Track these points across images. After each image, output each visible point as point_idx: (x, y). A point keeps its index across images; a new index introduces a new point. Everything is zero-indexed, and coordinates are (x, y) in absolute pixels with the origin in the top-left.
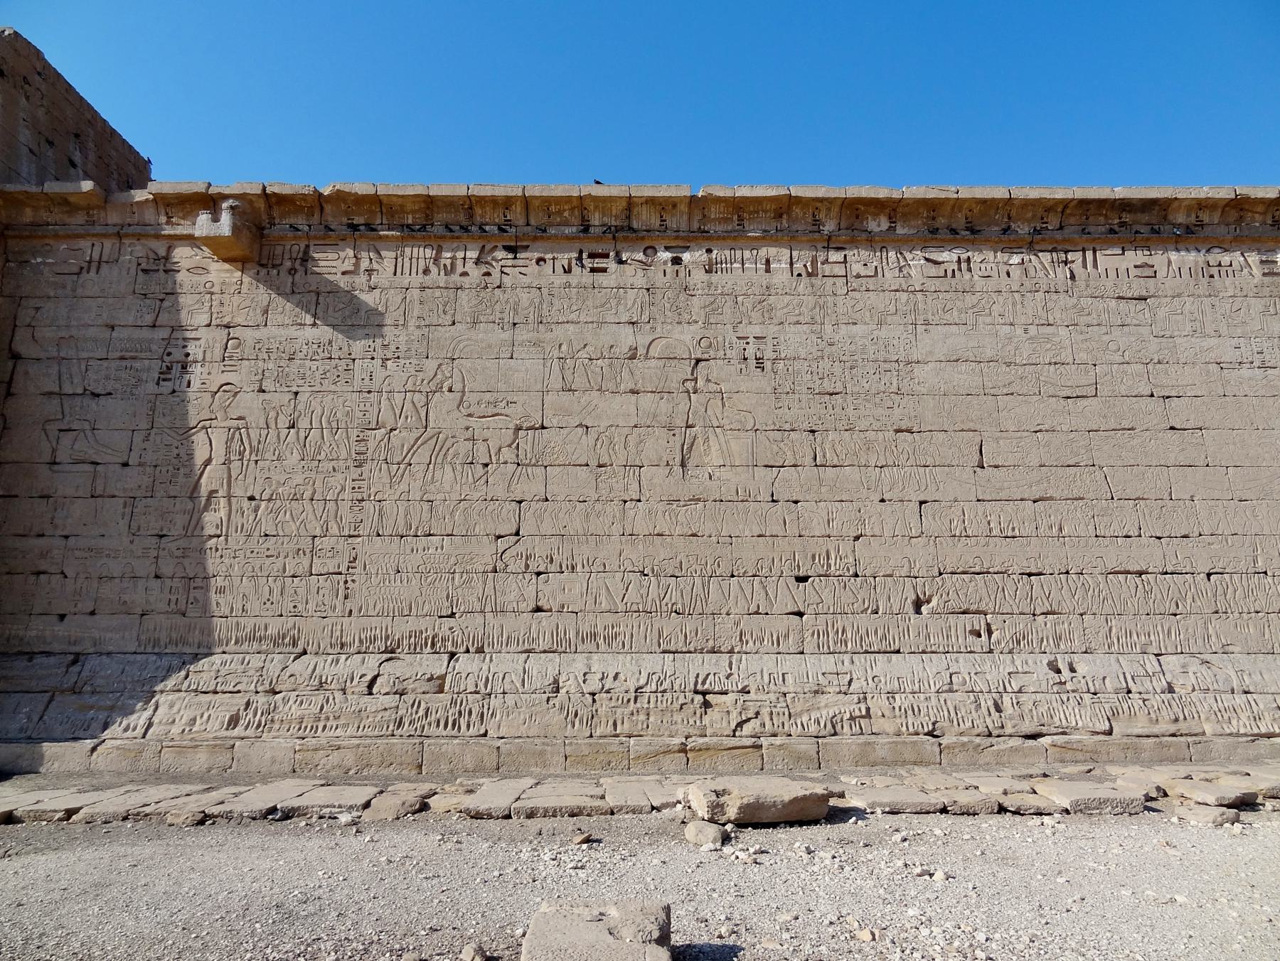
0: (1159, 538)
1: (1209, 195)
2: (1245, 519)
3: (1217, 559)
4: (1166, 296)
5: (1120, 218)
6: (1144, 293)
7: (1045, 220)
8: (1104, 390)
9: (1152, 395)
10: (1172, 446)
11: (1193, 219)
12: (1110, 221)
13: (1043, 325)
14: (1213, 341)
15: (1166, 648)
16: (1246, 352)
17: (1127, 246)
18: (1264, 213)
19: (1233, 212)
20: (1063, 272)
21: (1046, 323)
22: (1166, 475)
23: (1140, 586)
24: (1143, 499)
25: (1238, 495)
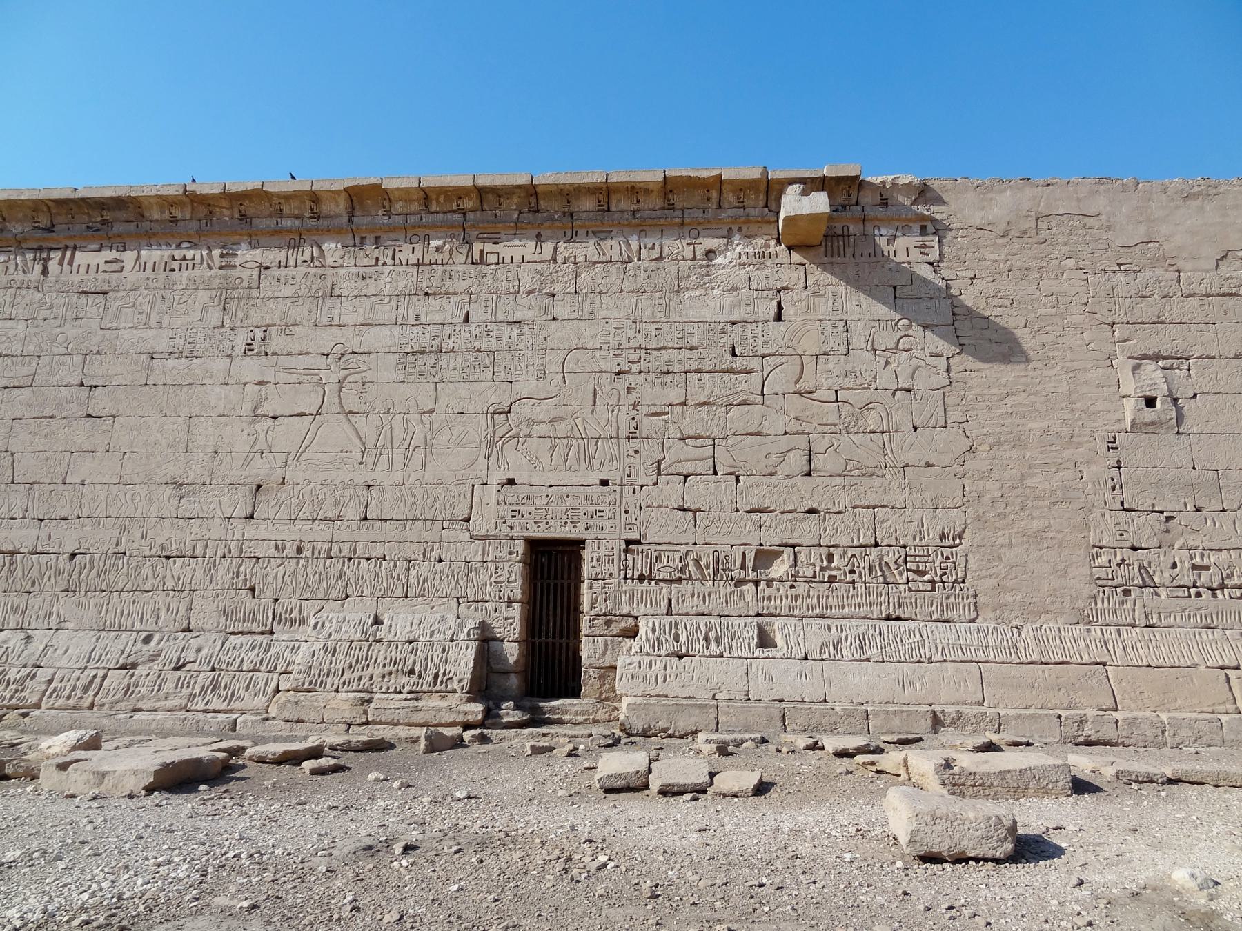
0: (42, 520)
1: (159, 193)
2: (123, 501)
3: (85, 540)
4: (125, 290)
5: (102, 217)
6: (106, 288)
7: (36, 220)
8: (39, 379)
9: (82, 385)
10: (80, 434)
11: (167, 215)
12: (93, 220)
13: (6, 319)
14: (151, 332)
15: (8, 624)
16: (179, 342)
17: (105, 243)
18: (231, 208)
19: (201, 208)
20: (38, 268)
21: (9, 317)
22: (67, 460)
23: (7, 565)
24: (39, 483)
25: (127, 479)
